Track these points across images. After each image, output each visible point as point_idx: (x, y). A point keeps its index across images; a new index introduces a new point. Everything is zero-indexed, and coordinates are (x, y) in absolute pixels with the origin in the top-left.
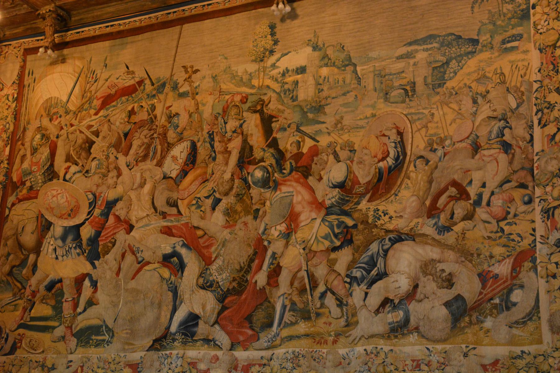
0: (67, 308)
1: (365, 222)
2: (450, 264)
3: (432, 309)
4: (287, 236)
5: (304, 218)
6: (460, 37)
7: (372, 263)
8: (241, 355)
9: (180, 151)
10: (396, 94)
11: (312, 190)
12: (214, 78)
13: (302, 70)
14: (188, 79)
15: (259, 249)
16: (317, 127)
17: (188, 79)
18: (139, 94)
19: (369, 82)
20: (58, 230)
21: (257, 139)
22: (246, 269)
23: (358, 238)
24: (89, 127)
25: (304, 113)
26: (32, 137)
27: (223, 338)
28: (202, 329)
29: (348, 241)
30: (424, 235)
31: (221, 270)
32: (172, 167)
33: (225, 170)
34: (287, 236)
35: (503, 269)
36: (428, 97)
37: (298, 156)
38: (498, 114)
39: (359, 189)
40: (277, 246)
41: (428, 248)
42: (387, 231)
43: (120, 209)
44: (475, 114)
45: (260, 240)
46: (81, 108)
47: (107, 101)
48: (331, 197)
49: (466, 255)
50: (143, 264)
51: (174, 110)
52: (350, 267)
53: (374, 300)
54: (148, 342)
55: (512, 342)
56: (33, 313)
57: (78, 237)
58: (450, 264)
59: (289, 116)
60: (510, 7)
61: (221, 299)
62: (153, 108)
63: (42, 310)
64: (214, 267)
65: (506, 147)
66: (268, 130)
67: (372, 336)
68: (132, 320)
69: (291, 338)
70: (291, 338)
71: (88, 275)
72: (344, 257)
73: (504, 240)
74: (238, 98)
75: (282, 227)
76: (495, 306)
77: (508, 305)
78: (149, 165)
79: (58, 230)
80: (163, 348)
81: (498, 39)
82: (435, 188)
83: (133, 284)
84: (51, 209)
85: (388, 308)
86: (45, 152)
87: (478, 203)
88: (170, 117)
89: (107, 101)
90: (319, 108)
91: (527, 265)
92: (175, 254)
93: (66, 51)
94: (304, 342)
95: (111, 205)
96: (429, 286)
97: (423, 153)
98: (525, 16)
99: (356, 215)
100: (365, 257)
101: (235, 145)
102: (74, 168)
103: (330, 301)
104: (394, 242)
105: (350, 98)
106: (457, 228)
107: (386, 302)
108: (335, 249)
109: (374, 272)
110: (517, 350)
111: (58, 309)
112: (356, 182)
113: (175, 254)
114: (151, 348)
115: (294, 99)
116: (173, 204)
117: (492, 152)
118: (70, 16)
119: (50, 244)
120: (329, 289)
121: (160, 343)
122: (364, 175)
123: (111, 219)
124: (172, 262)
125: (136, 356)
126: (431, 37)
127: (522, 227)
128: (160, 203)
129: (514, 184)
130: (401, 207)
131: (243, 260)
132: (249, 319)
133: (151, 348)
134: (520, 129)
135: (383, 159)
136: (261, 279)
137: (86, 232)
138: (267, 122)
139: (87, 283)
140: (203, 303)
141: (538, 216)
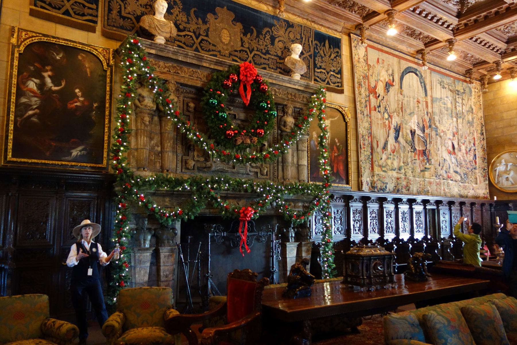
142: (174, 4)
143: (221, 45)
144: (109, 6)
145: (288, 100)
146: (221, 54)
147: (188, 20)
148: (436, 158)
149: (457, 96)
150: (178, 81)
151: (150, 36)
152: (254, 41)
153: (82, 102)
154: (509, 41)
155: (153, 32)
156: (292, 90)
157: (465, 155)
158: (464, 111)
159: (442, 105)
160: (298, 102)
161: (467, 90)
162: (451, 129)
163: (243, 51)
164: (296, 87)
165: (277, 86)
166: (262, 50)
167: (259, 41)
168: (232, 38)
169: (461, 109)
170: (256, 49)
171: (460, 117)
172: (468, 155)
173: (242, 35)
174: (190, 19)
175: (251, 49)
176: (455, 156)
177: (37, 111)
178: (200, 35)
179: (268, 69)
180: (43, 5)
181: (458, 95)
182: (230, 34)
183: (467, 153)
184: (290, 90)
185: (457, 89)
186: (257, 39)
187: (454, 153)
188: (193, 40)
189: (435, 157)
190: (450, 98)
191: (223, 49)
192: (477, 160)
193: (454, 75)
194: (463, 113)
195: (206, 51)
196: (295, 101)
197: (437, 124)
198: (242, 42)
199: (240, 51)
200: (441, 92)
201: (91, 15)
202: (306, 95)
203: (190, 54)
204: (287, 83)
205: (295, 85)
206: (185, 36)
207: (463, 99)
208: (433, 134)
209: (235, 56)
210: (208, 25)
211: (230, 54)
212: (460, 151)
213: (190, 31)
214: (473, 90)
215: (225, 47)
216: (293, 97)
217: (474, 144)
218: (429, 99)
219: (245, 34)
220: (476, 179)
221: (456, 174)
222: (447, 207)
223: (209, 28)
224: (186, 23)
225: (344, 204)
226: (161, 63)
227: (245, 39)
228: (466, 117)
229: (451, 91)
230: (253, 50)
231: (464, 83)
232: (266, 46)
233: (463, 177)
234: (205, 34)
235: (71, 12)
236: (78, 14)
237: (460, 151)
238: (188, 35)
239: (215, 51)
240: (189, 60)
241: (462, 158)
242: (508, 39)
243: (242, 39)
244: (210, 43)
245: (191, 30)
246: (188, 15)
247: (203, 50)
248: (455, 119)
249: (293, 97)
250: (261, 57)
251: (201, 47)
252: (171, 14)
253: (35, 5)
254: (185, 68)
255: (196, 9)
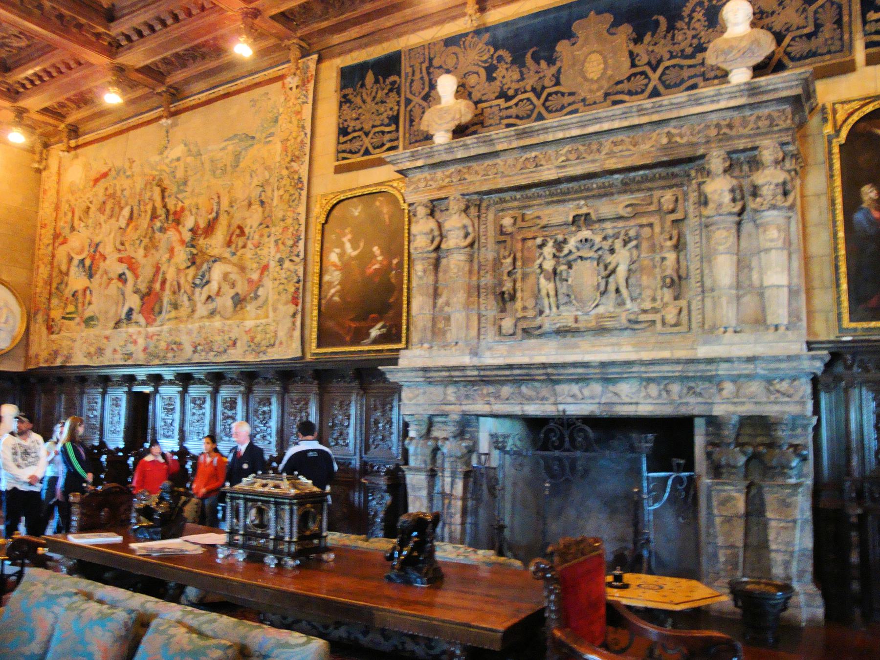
0: (80, 305)
1: (201, 251)
2: (234, 276)
3: (225, 302)
4: (169, 260)
5: (176, 250)
6: (247, 135)
7: (203, 276)
8: (151, 330)
9: (126, 212)
10: (219, 172)
11: (180, 233)
12: (142, 165)
13: (178, 159)
14: (130, 168)
15: (158, 269)
16: (185, 194)
17: (130, 168)
18: (109, 178)
19: (208, 166)
20: (76, 262)
21: (159, 204)
22: (153, 281)
23: (198, 261)
24: (88, 198)
25: (178, 186)
26: (65, 207)
27: (142, 321)
28: (135, 316)
29: (194, 263)
30: (225, 258)
31: (142, 282)
32: (123, 223)
33: (144, 222)
34: (169, 260)
35: (255, 276)
36: (232, 173)
37: (175, 213)
38: (259, 183)
39: (200, 232)
40: (164, 268)
41: (227, 265)
42: (211, 256)
43: (101, 249)
44: (250, 184)
45: (158, 263)
46: (85, 187)
47: (96, 181)
48: (187, 236)
49: (242, 269)
50: (111, 279)
51: (124, 187)
52: (194, 278)
53: (204, 297)
54: (112, 324)
55: (256, 318)
56: (68, 310)
57: (84, 266)
58: (234, 276)
59: (172, 189)
60: (270, 115)
61: (142, 299)
62: (115, 185)
63: (71, 308)
64: (139, 280)
65: (262, 203)
66: (163, 198)
67: (202, 318)
68: (106, 312)
69: (169, 319)
70: (169, 319)
71: (88, 288)
72: (192, 271)
73: (256, 260)
74: (151, 178)
75: (167, 256)
76: (251, 298)
77: (257, 297)
78: (113, 221)
79: (76, 262)
80: (119, 327)
81: (264, 135)
82: (231, 231)
83: (106, 292)
84: (72, 249)
85: (210, 301)
86: (70, 215)
87: (248, 239)
88: (123, 191)
89: (96, 181)
90: (185, 183)
91: (266, 273)
92: (124, 274)
93: (79, 151)
94: (174, 322)
95: (97, 245)
96: (226, 288)
97: (227, 209)
98: (276, 121)
99: (198, 247)
100: (200, 273)
101: (149, 208)
102: (82, 224)
103: (185, 298)
104: (215, 261)
105: (198, 175)
106: (238, 254)
107: (209, 297)
108: (188, 267)
109: (204, 281)
110: (258, 322)
111: (76, 307)
112: (198, 227)
113: (124, 274)
114: (115, 328)
115: (175, 177)
116: (122, 244)
117: (256, 207)
118: (78, 128)
119: (74, 270)
120: (185, 292)
121: (117, 325)
122: (202, 224)
123: (98, 254)
124: (121, 277)
125: (108, 332)
126: (236, 135)
127: (265, 252)
128: (118, 243)
129: (264, 226)
130: (215, 244)
131: (151, 275)
132: (153, 309)
133: (115, 328)
134: (269, 193)
135: (211, 213)
136: (157, 286)
137: (88, 262)
138: (163, 191)
139: (88, 292)
140: (134, 301)
141: (272, 245)
142: (499, 62)
143: (586, 86)
144: (411, 116)
145: (707, 142)
146: (587, 103)
147: (522, 74)
150: (466, 192)
151: (428, 137)
152: (663, 41)
153: (381, 262)
155: (431, 133)
156: (719, 114)
160: (740, 137)
163: (635, 75)
164: (723, 104)
165: (673, 123)
166: (683, 51)
167: (674, 35)
168: (610, 61)
170: (667, 56)
173: (631, 46)
174: (525, 70)
175: (654, 62)
177: (338, 287)
178: (544, 88)
179: (702, 84)
180: (345, 155)
182: (604, 58)
184: (714, 117)
186: (670, 35)
188: (532, 103)
191: (591, 91)
195: (556, 111)
196: (731, 138)
198: (632, 56)
199: (629, 79)
201: (391, 141)
202: (764, 111)
203: (469, 142)
204: (692, 105)
205: (718, 101)
206: (516, 104)
209: (618, 93)
210: (558, 64)
211: (607, 95)
213: (525, 92)
215: (595, 87)
216: (725, 130)
219: (638, 40)
223: (560, 68)
224: (518, 81)
226: (439, 173)
227: (639, 49)
230: (659, 62)
232: (694, 37)
234: (553, 83)
235: (370, 148)
236: (378, 147)
238: (522, 100)
239: (574, 103)
240: (473, 152)
243: (631, 54)
244: (563, 94)
245: (529, 88)
246: (522, 65)
247: (550, 112)
249: (725, 130)
250: (681, 67)
251: (547, 108)
252: (495, 79)
253: (338, 160)
254: (474, 165)
255: (535, 49)
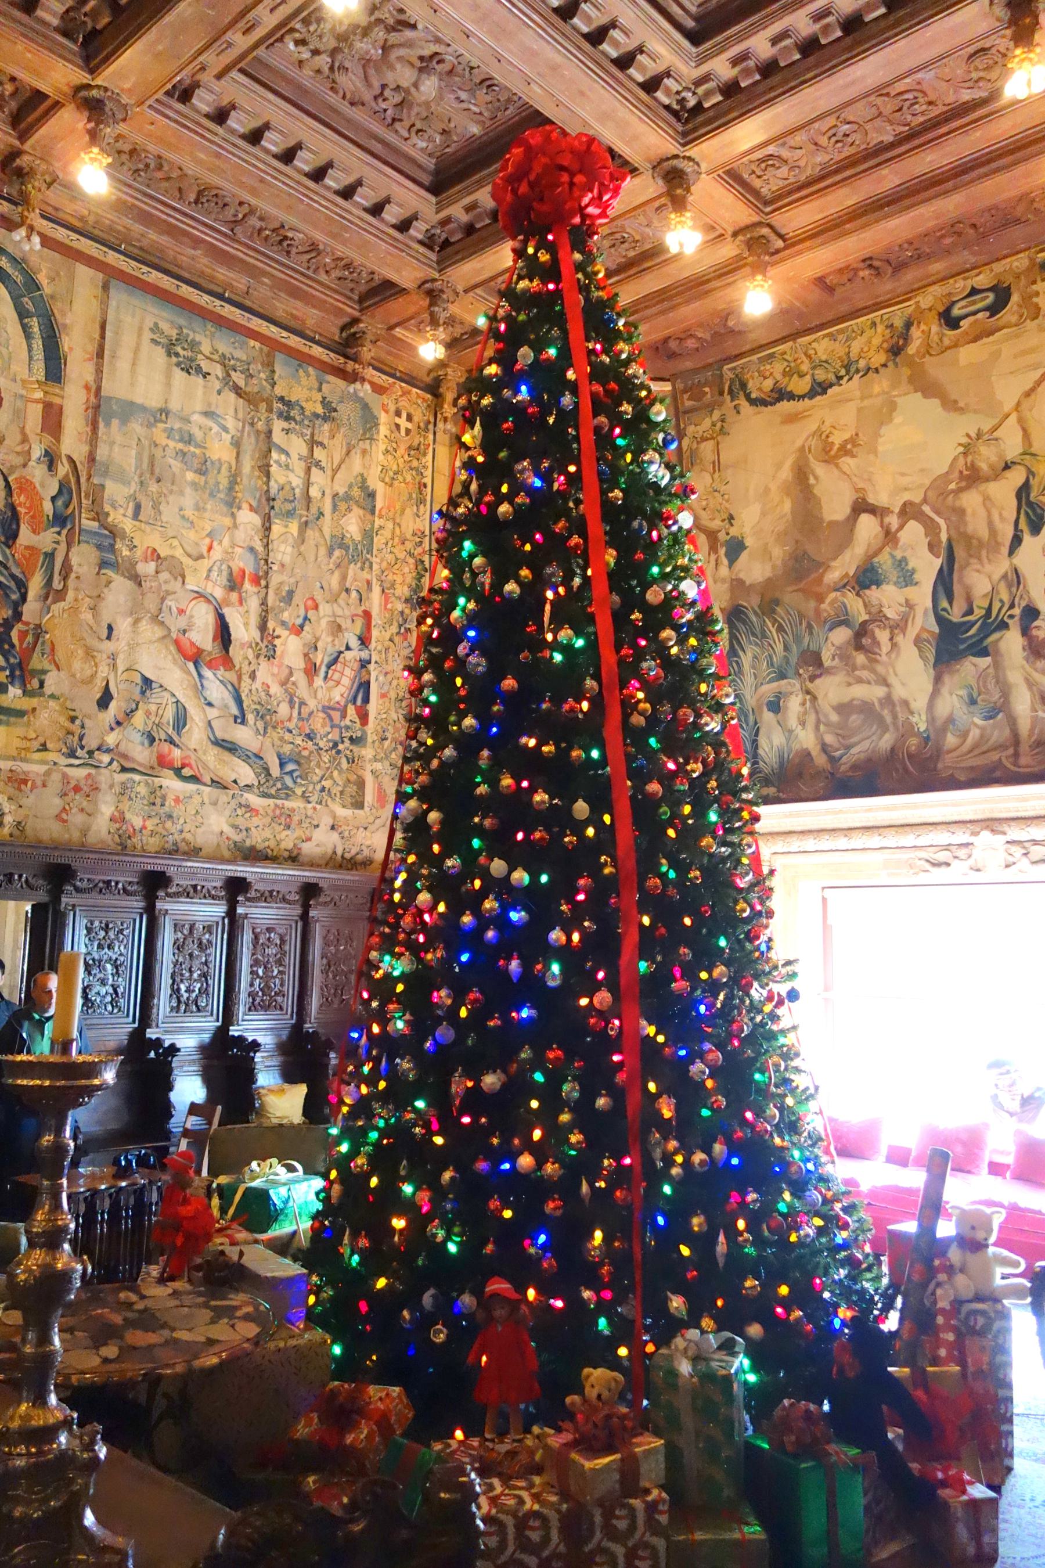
148: (79, 666)
149: (278, 425)
154: (442, 181)
157: (299, 677)
158: (314, 492)
159: (162, 440)
161: (346, 411)
162: (217, 554)
169: (297, 481)
171: (290, 514)
172: (319, 681)
176: (231, 676)
181: (288, 418)
183: (311, 670)
185: (279, 391)
187: (227, 662)
189: (77, 665)
190: (230, 423)
192: (373, 707)
193: (273, 331)
194: (308, 499)
197: (121, 518)
200: (168, 385)
207: (313, 443)
208: (83, 558)
212: (271, 656)
214: (383, 418)
217: (364, 641)
218: (73, 400)
220: (361, 784)
221: (226, 756)
222: (138, 903)
225: (142, 904)
228: (327, 522)
229: (238, 390)
231: (330, 378)
233: (275, 771)
237: (271, 656)
241: (275, 689)
242: (437, 172)
248: (248, 519)
